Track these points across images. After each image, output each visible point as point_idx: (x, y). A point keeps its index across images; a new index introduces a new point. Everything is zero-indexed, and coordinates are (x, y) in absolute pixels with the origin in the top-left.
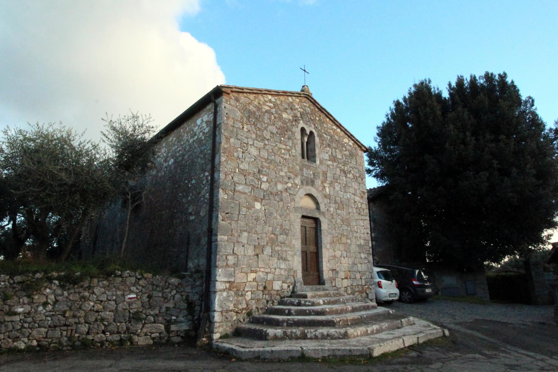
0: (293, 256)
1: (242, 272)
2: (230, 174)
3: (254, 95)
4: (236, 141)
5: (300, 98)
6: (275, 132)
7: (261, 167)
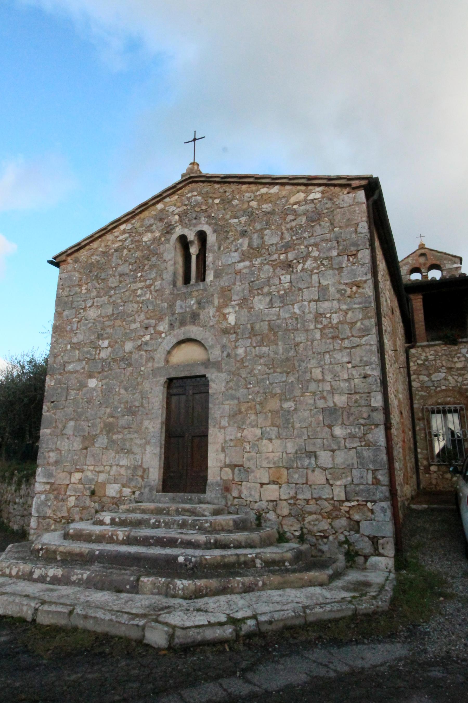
0: (143, 446)
1: (64, 471)
2: (60, 355)
3: (100, 240)
4: (71, 311)
5: (179, 192)
6: (128, 271)
7: (102, 329)
